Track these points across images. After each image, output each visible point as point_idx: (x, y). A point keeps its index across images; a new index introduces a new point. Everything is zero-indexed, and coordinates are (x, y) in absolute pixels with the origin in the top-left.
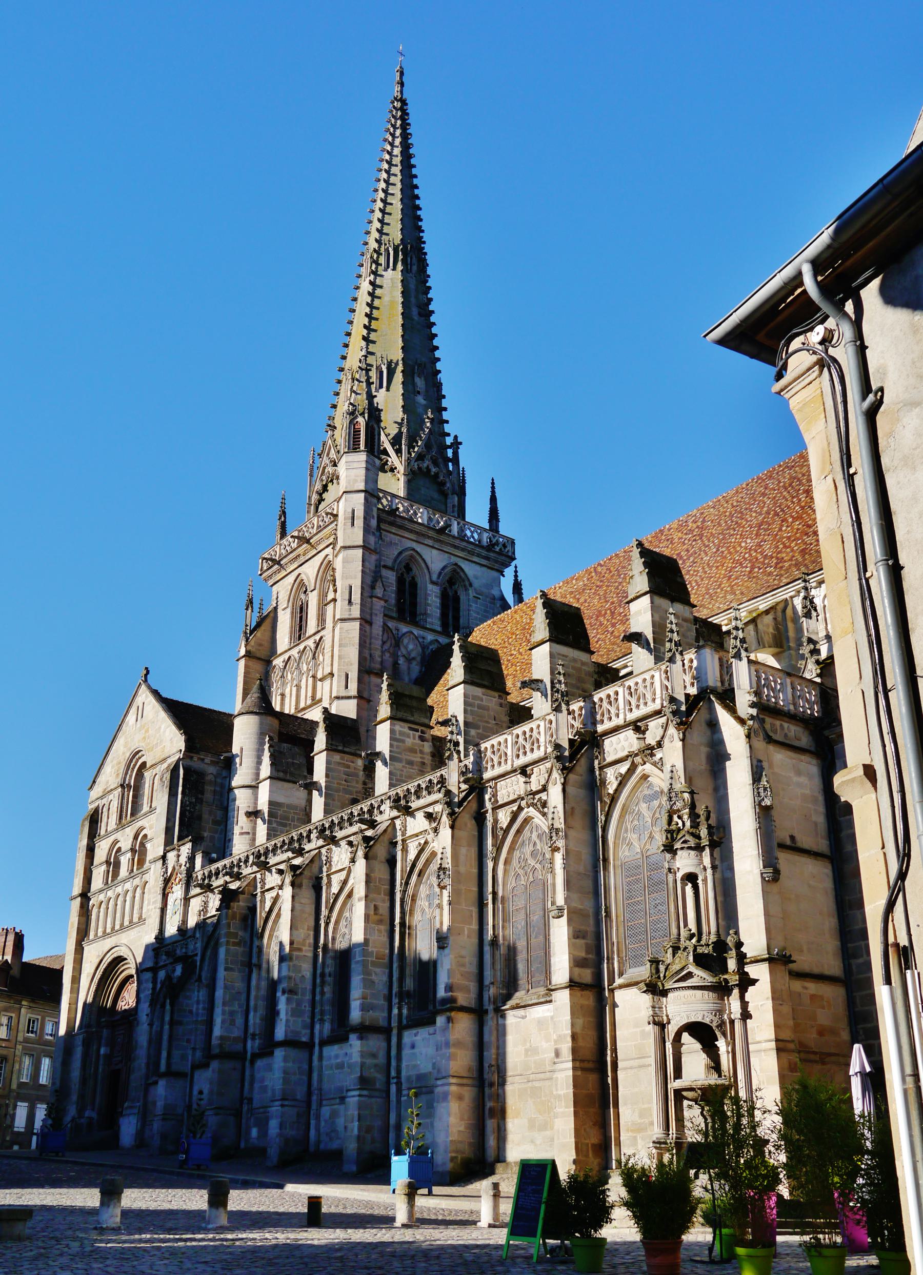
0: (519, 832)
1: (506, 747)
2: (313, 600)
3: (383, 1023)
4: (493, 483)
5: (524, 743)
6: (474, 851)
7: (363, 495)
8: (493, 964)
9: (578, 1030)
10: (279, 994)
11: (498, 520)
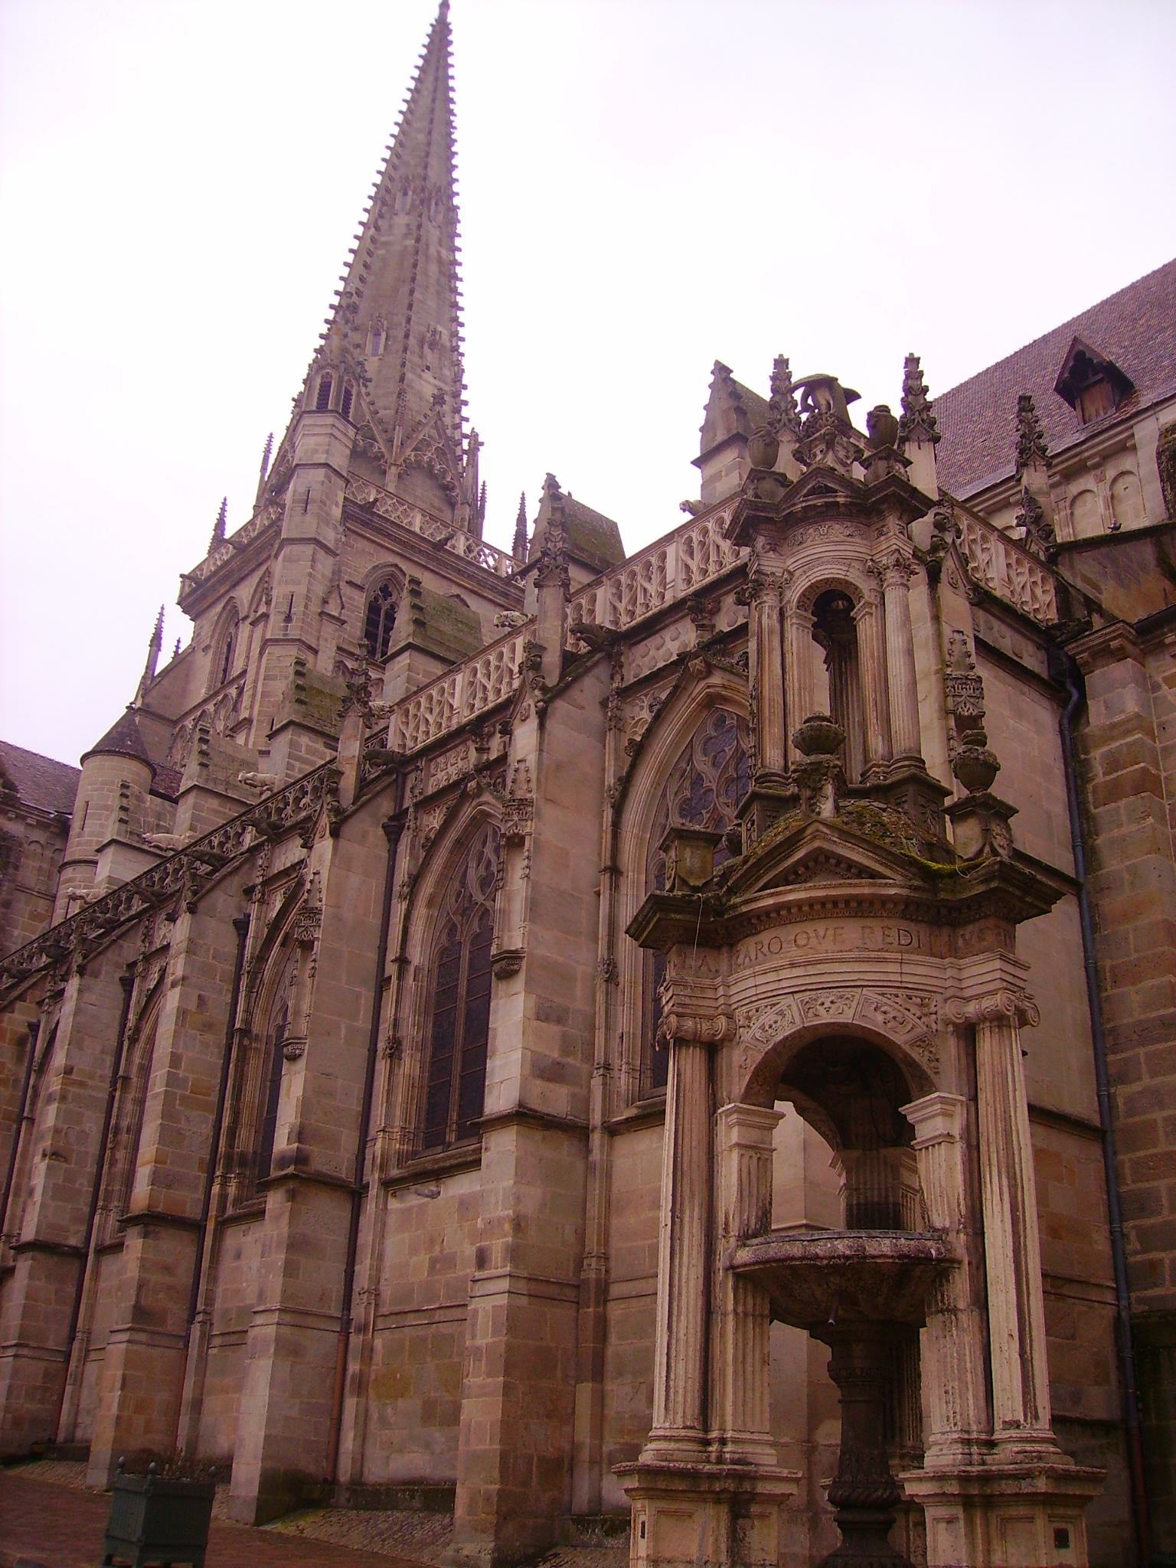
0: (460, 844)
1: (453, 695)
3: (193, 1211)
4: (523, 499)
5: (484, 681)
7: (322, 471)
8: (389, 1092)
9: (530, 1207)
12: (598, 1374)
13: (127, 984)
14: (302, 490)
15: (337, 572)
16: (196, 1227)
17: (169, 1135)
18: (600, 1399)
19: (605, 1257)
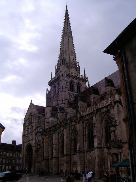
0: (89, 124)
2: (57, 89)
6: (82, 127)
10: (53, 150)
12: (104, 165)
13: (59, 134)
14: (62, 74)
15: (66, 82)
16: (70, 155)
17: (67, 148)
18: (105, 167)
19: (104, 157)
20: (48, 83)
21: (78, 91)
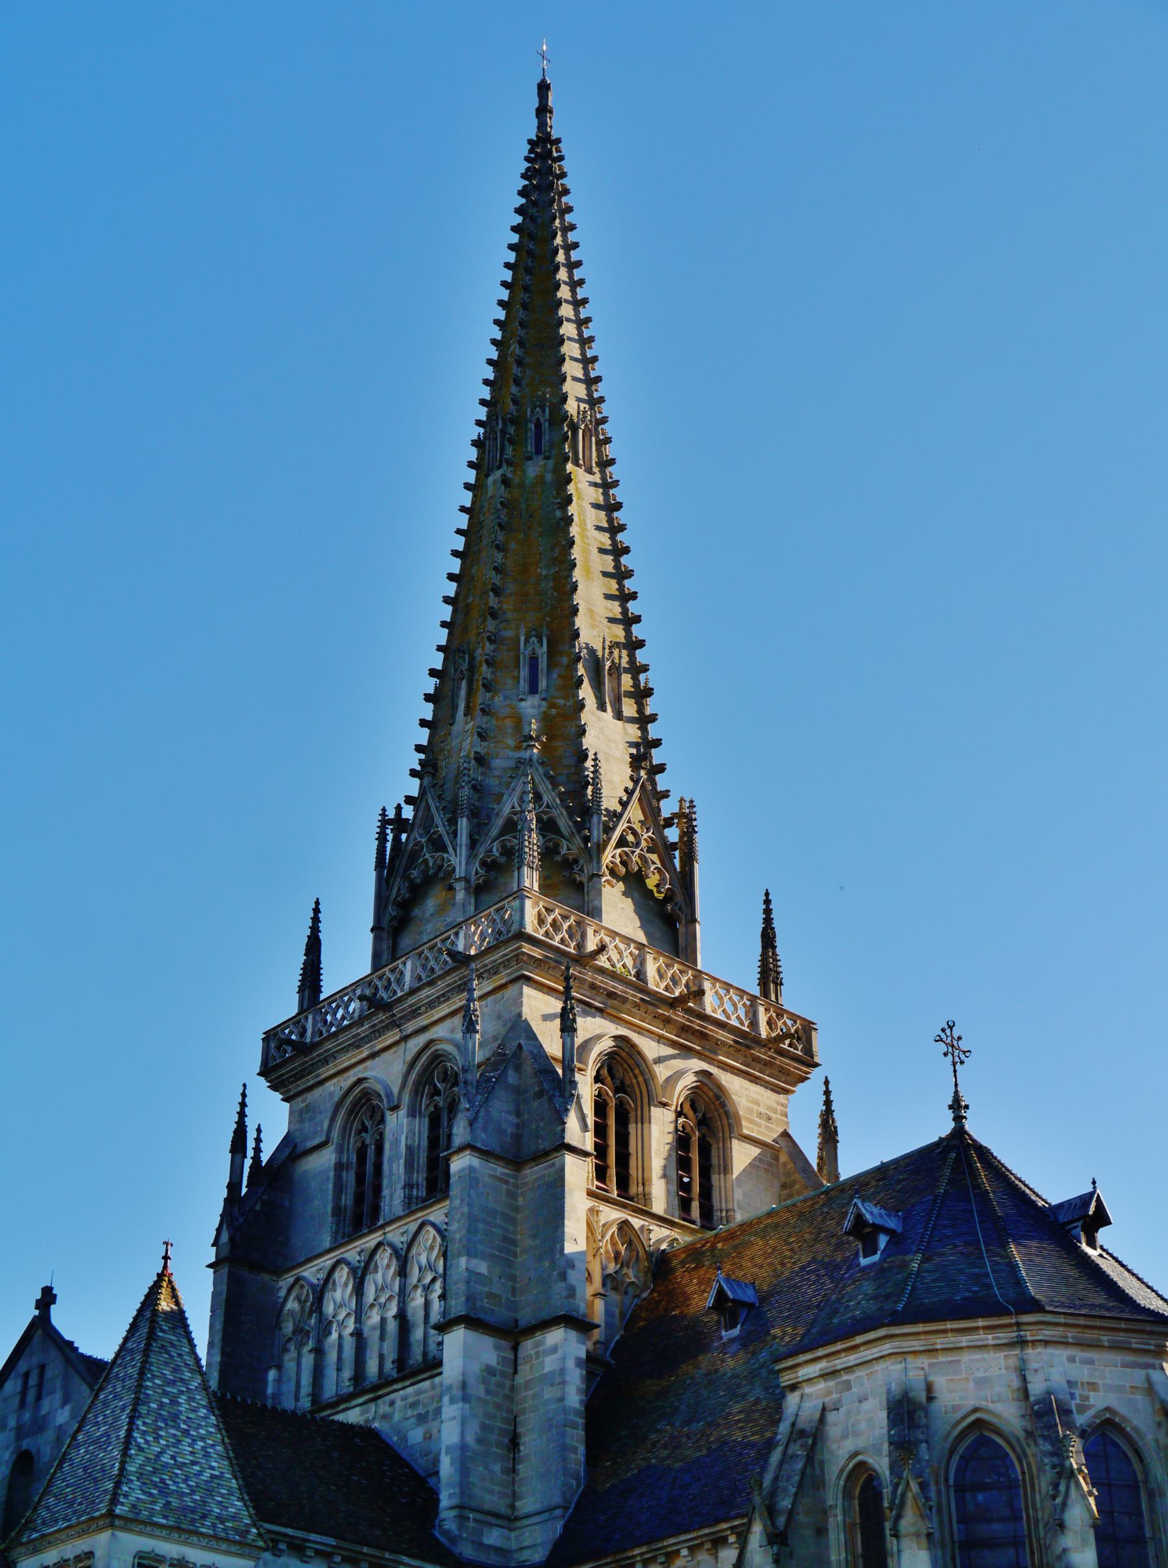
11: (778, 983)
20: (255, 1060)
21: (685, 1205)
